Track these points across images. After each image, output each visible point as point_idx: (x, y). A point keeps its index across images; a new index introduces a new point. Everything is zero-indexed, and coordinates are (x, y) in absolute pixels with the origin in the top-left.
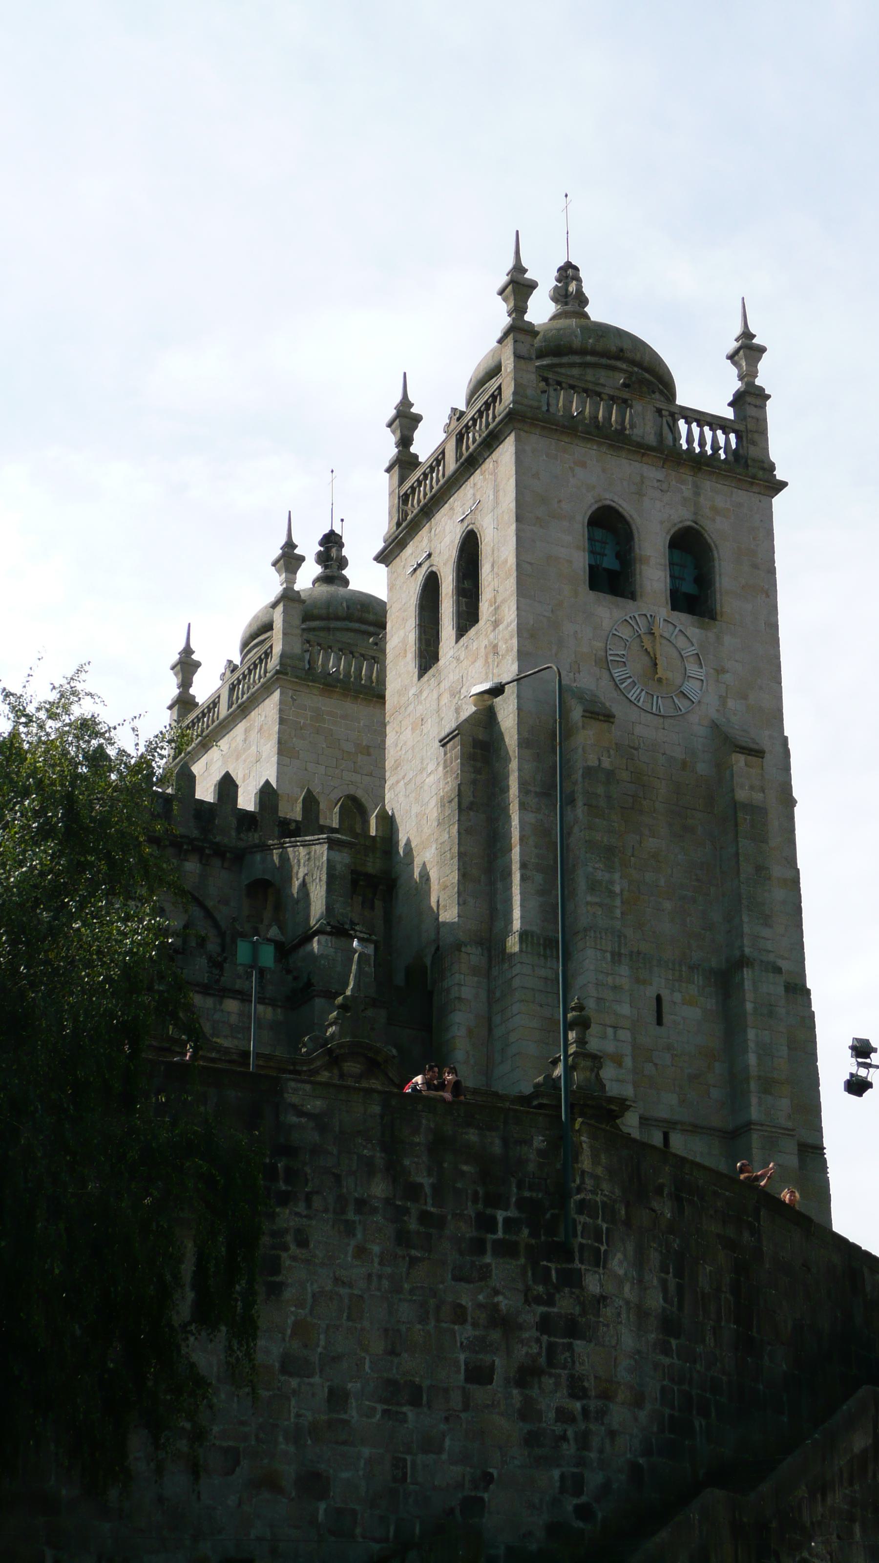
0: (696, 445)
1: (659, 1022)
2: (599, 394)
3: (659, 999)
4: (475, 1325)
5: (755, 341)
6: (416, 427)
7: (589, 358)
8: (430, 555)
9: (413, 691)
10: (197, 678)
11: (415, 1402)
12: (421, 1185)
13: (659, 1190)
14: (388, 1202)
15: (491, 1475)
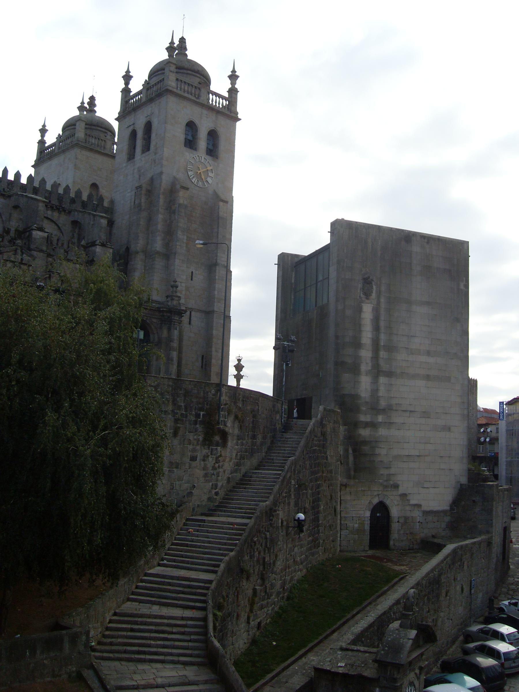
0: (217, 104)
1: (192, 280)
2: (192, 86)
3: (192, 272)
4: (193, 445)
5: (236, 74)
6: (131, 79)
7: (189, 72)
8: (134, 124)
9: (124, 165)
10: (47, 135)
11: (177, 467)
12: (181, 406)
13: (239, 400)
14: (173, 411)
15: (195, 485)
